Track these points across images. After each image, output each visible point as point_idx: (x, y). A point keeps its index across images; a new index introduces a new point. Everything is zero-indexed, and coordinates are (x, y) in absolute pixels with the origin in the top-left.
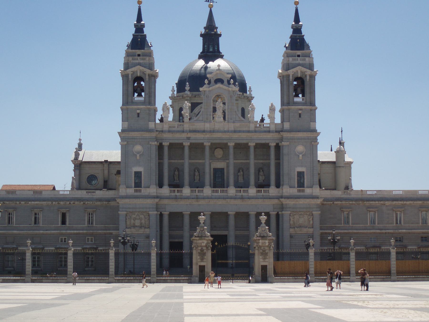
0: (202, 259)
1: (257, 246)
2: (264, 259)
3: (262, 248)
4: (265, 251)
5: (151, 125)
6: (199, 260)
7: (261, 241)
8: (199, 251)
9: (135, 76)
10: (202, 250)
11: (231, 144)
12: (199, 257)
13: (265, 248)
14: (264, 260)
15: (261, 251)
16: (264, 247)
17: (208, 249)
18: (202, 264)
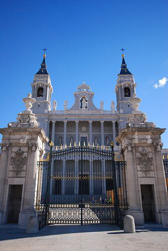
0: (17, 172)
1: (130, 144)
2: (147, 171)
3: (140, 149)
4: (146, 154)
5: (46, 111)
6: (11, 174)
7: (136, 136)
8: (13, 155)
9: (38, 86)
10: (19, 154)
11: (91, 122)
12: (11, 168)
13: (145, 148)
14: (146, 174)
15: (138, 155)
16: (143, 147)
17: (32, 151)
18: (17, 181)
